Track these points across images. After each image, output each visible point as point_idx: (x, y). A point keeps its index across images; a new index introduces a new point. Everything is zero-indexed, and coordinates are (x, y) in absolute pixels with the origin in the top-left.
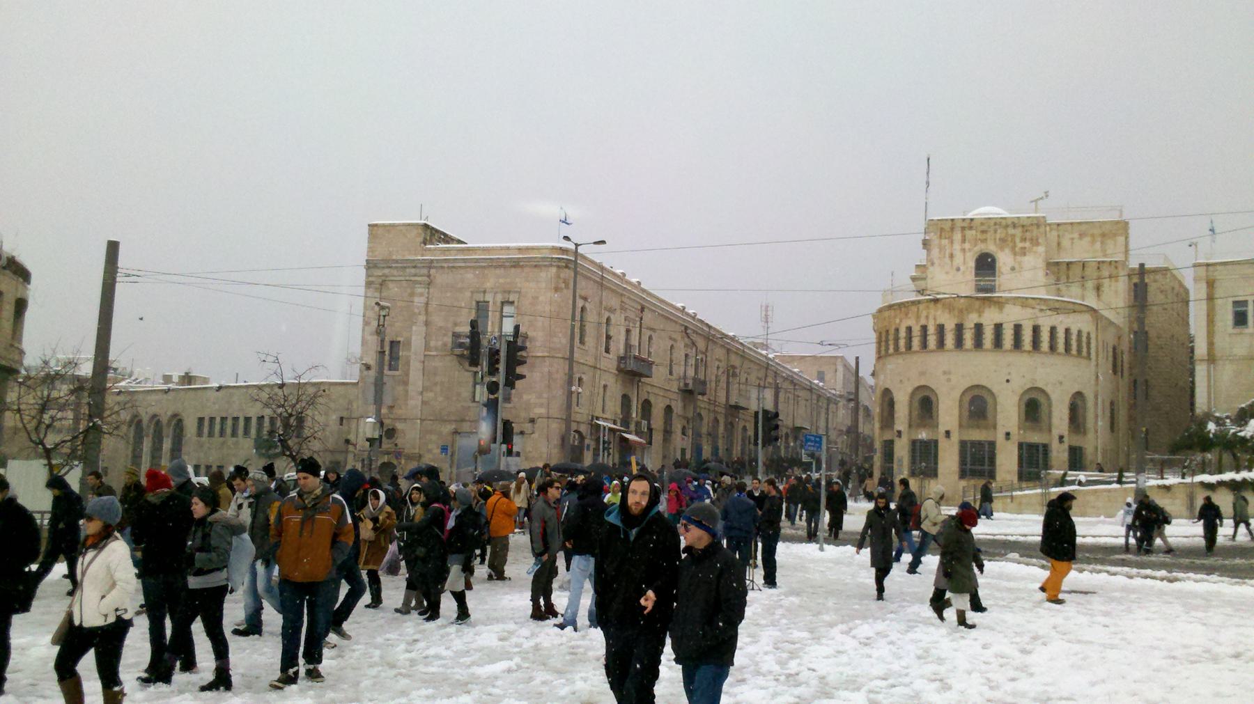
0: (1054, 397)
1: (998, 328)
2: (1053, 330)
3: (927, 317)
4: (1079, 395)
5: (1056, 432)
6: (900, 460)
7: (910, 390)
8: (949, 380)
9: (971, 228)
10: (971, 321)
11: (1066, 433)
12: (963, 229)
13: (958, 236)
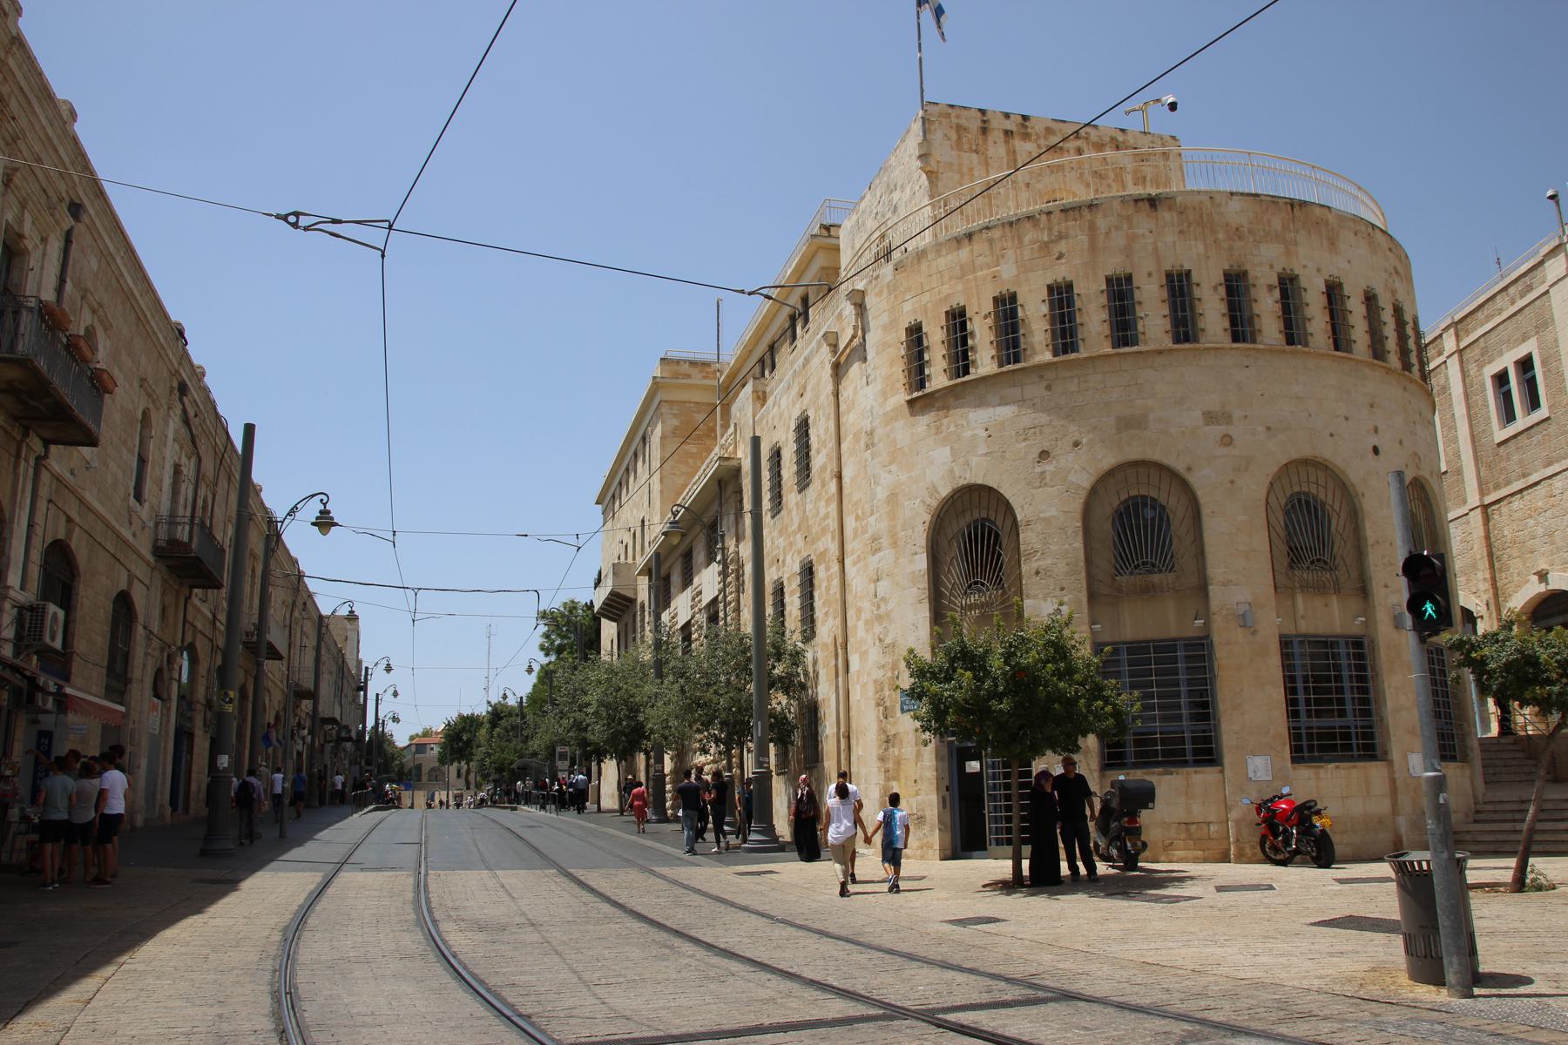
3: (1128, 251)
8: (1227, 441)
9: (1026, 136)
13: (997, 150)
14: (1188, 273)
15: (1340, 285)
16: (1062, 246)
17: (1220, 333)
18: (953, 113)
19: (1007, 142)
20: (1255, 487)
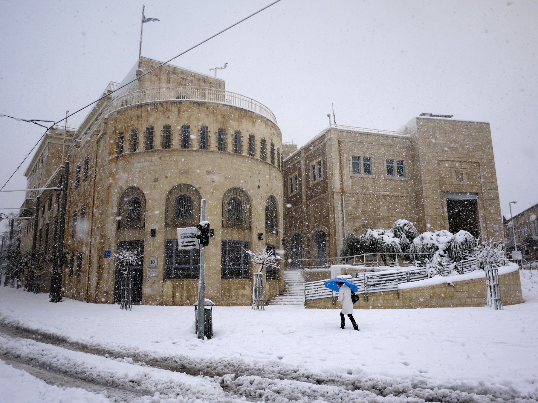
3: (189, 118)
9: (174, 73)
13: (164, 77)
14: (207, 128)
15: (254, 137)
16: (169, 114)
17: (215, 147)
20: (220, 194)
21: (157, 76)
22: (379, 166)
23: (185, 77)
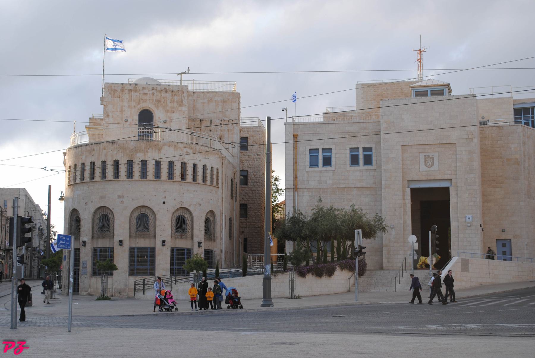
0: (195, 214)
1: (158, 164)
2: (195, 166)
3: (106, 155)
4: (211, 212)
5: (196, 240)
6: (85, 263)
7: (93, 210)
9: (136, 91)
10: (138, 158)
11: (202, 240)
12: (130, 91)
13: (126, 96)
18: (113, 85)
19: (129, 93)
20: (128, 213)
21: (119, 97)
22: (341, 157)
23: (146, 91)
